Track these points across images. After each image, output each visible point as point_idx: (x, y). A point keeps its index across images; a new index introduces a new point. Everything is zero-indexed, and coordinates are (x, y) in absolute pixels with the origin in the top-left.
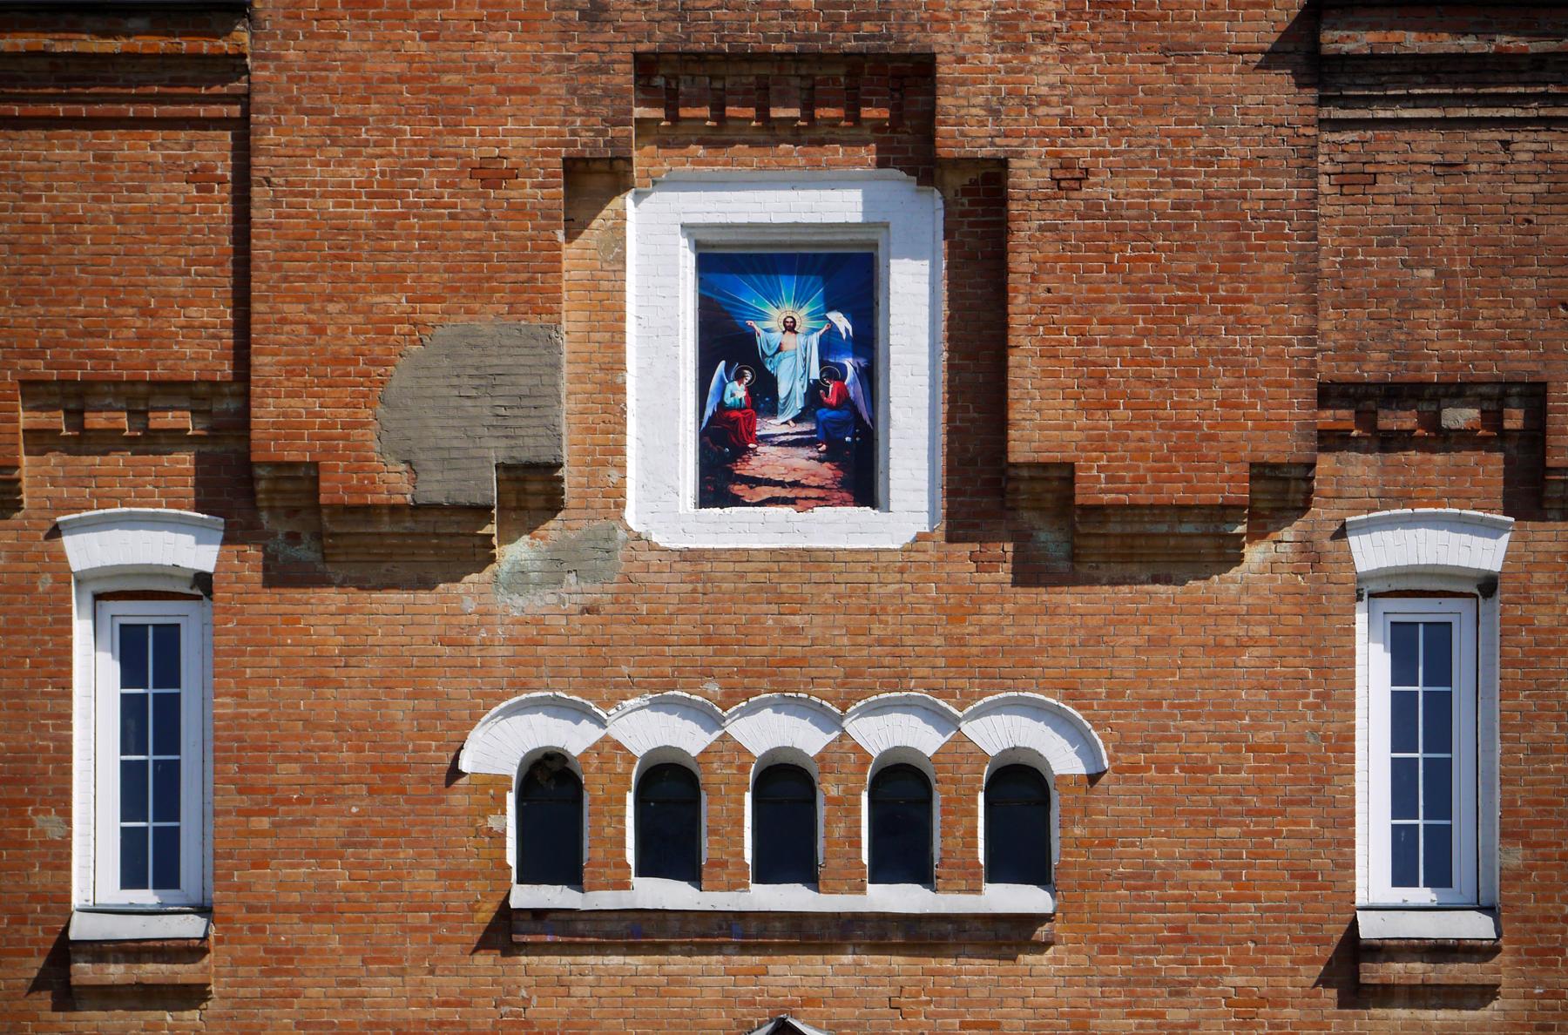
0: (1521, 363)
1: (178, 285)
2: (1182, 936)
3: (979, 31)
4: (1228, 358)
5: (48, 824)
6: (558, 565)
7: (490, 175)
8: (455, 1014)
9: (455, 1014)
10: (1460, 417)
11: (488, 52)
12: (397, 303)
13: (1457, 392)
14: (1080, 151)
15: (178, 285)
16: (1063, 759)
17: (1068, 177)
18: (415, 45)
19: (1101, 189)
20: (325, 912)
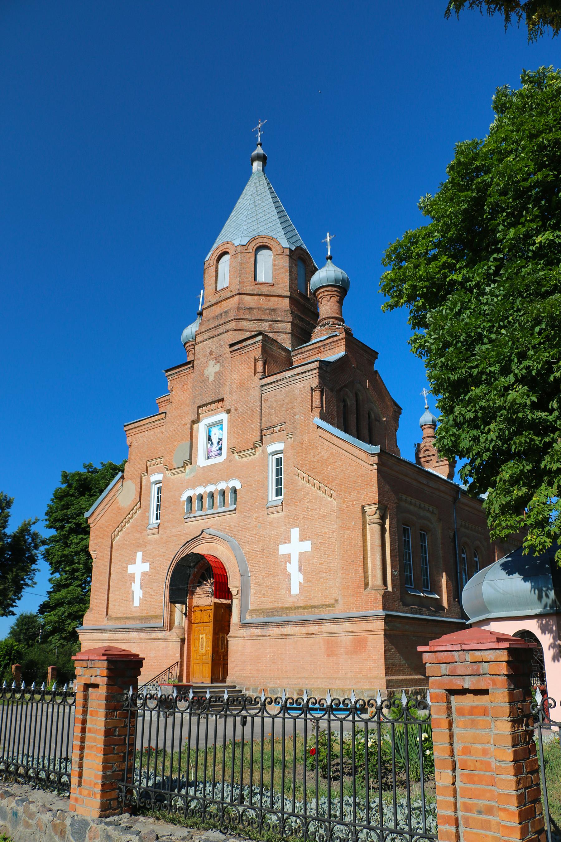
0: (283, 420)
1: (159, 446)
2: (249, 510)
3: (228, 393)
4: (252, 428)
5: (147, 514)
6: (191, 471)
7: (184, 425)
8: (180, 533)
9: (180, 533)
10: (278, 428)
11: (185, 410)
12: (176, 443)
13: (276, 425)
14: (238, 406)
15: (159, 446)
16: (238, 486)
17: (236, 409)
18: (179, 412)
19: (239, 410)
20: (169, 521)
